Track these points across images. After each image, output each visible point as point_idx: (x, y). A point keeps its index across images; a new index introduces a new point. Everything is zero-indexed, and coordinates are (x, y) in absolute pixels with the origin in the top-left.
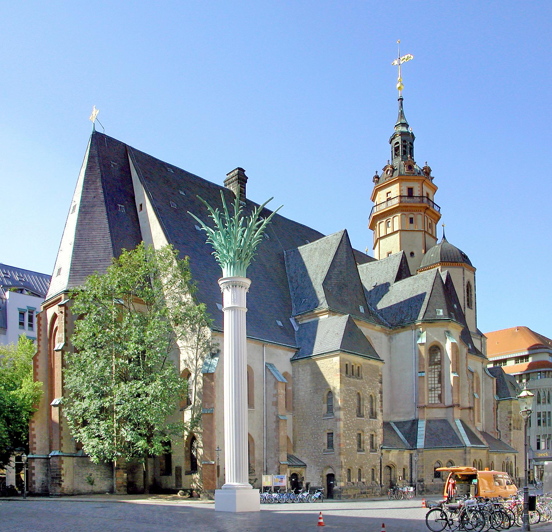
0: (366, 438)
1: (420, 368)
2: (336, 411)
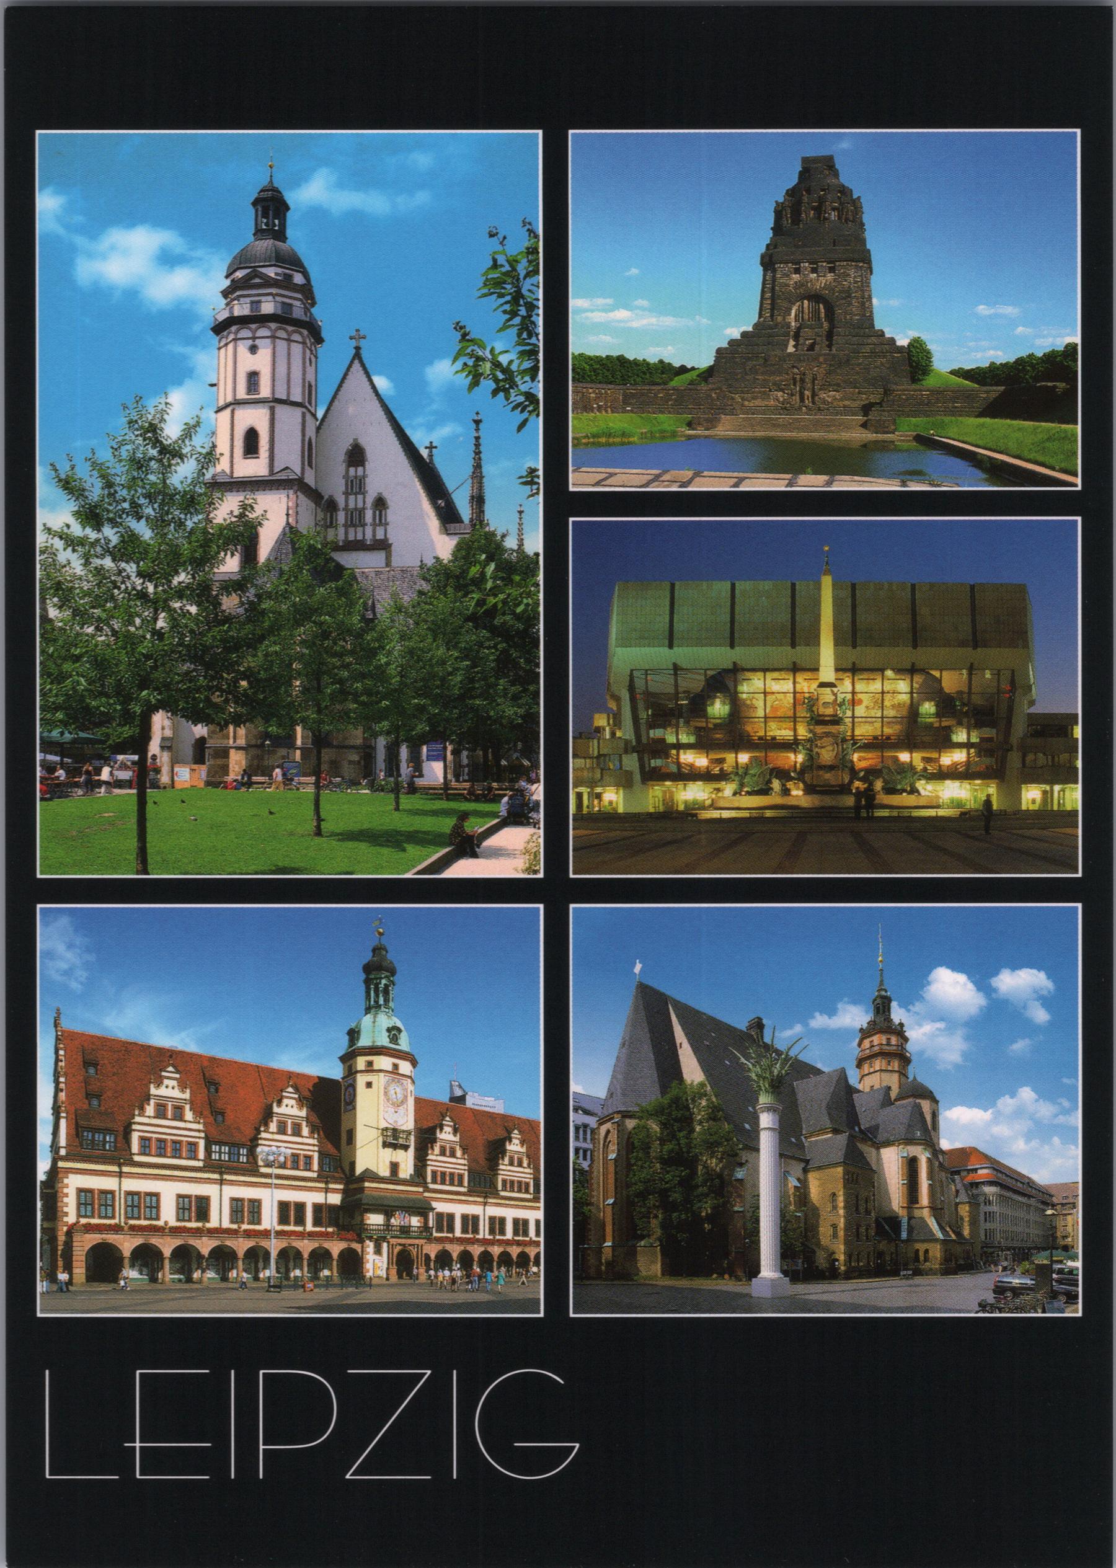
0: (863, 1230)
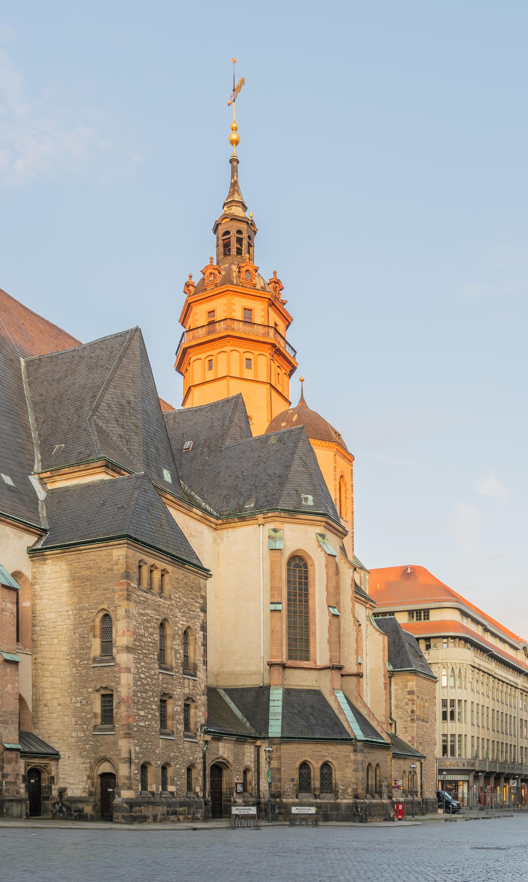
1: (272, 596)
2: (118, 653)
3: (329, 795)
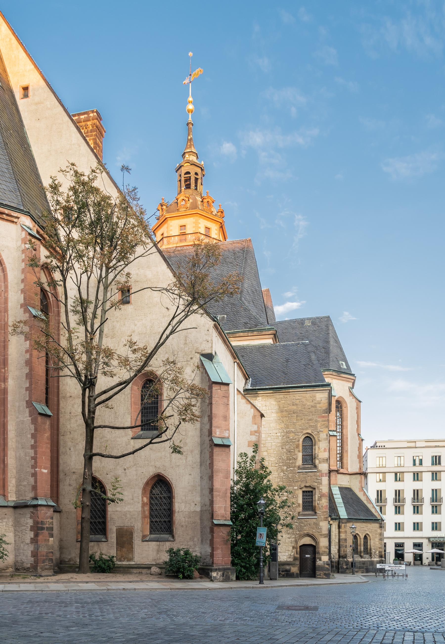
3: (367, 556)
